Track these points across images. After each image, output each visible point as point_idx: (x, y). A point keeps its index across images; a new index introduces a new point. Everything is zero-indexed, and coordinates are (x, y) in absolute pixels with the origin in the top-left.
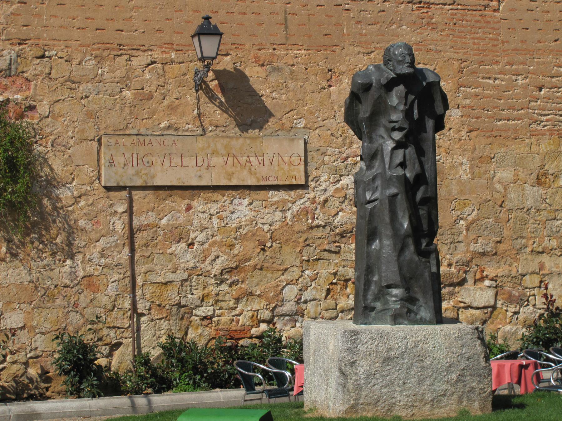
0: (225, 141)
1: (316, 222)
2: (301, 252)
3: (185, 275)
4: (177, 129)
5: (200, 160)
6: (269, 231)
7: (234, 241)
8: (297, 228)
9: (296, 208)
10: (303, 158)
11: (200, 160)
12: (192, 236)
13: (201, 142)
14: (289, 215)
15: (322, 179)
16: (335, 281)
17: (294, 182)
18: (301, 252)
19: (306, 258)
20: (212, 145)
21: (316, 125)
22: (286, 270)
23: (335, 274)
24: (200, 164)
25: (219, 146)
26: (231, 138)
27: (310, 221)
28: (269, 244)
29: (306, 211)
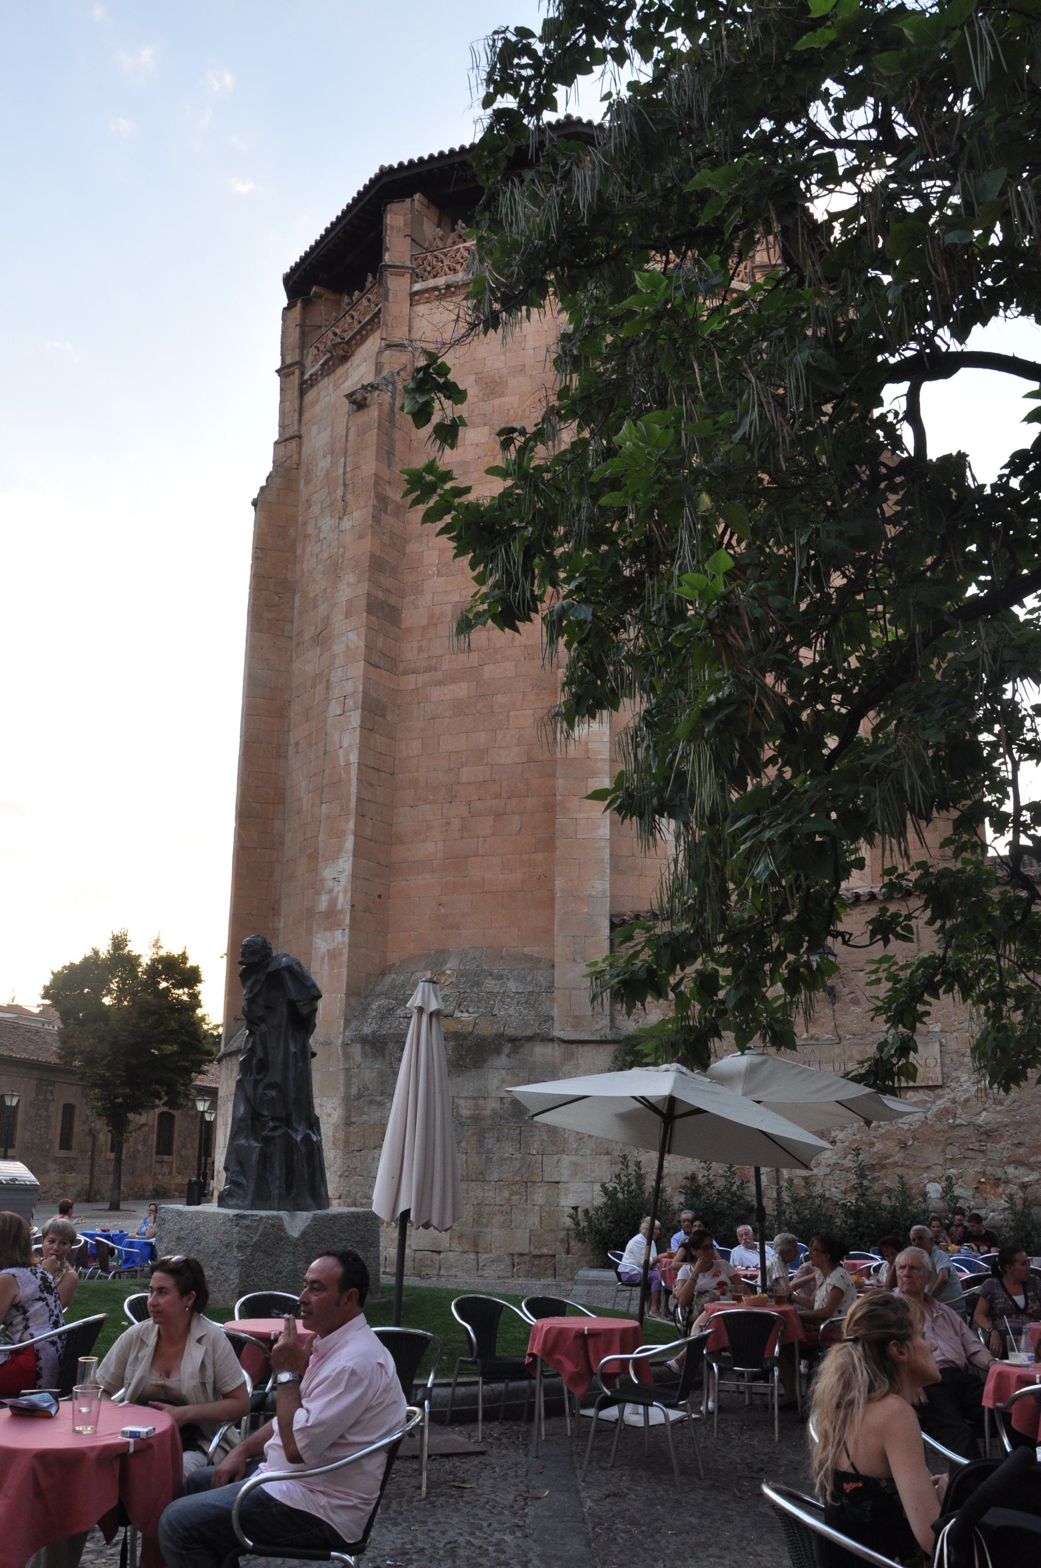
0: (860, 1048)
1: (958, 1121)
2: (944, 1151)
3: (828, 1170)
4: (817, 1039)
5: (837, 1065)
6: (909, 1130)
7: (875, 1140)
8: (939, 1126)
9: (935, 1108)
10: (939, 1060)
11: (837, 1065)
12: (834, 1134)
13: (837, 1050)
14: (929, 1115)
15: (962, 1080)
16: (983, 1180)
17: (931, 1083)
18: (944, 1151)
19: (949, 1157)
20: (848, 1053)
21: (953, 1028)
22: (929, 1167)
23: (984, 1174)
24: (837, 1069)
25: (854, 1052)
26: (866, 1044)
27: (951, 1121)
28: (910, 1143)
29: (945, 1112)
